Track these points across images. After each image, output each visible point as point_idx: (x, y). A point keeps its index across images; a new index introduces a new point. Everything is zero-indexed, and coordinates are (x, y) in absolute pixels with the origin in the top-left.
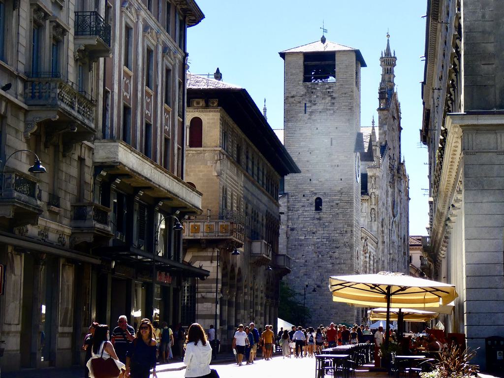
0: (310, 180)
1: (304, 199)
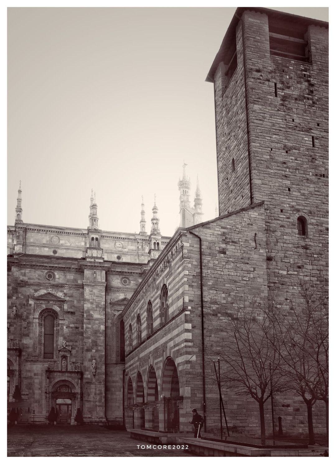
0: (289, 190)
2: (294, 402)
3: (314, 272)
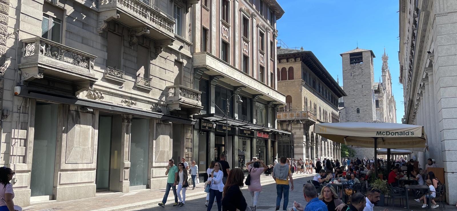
1: (352, 109)
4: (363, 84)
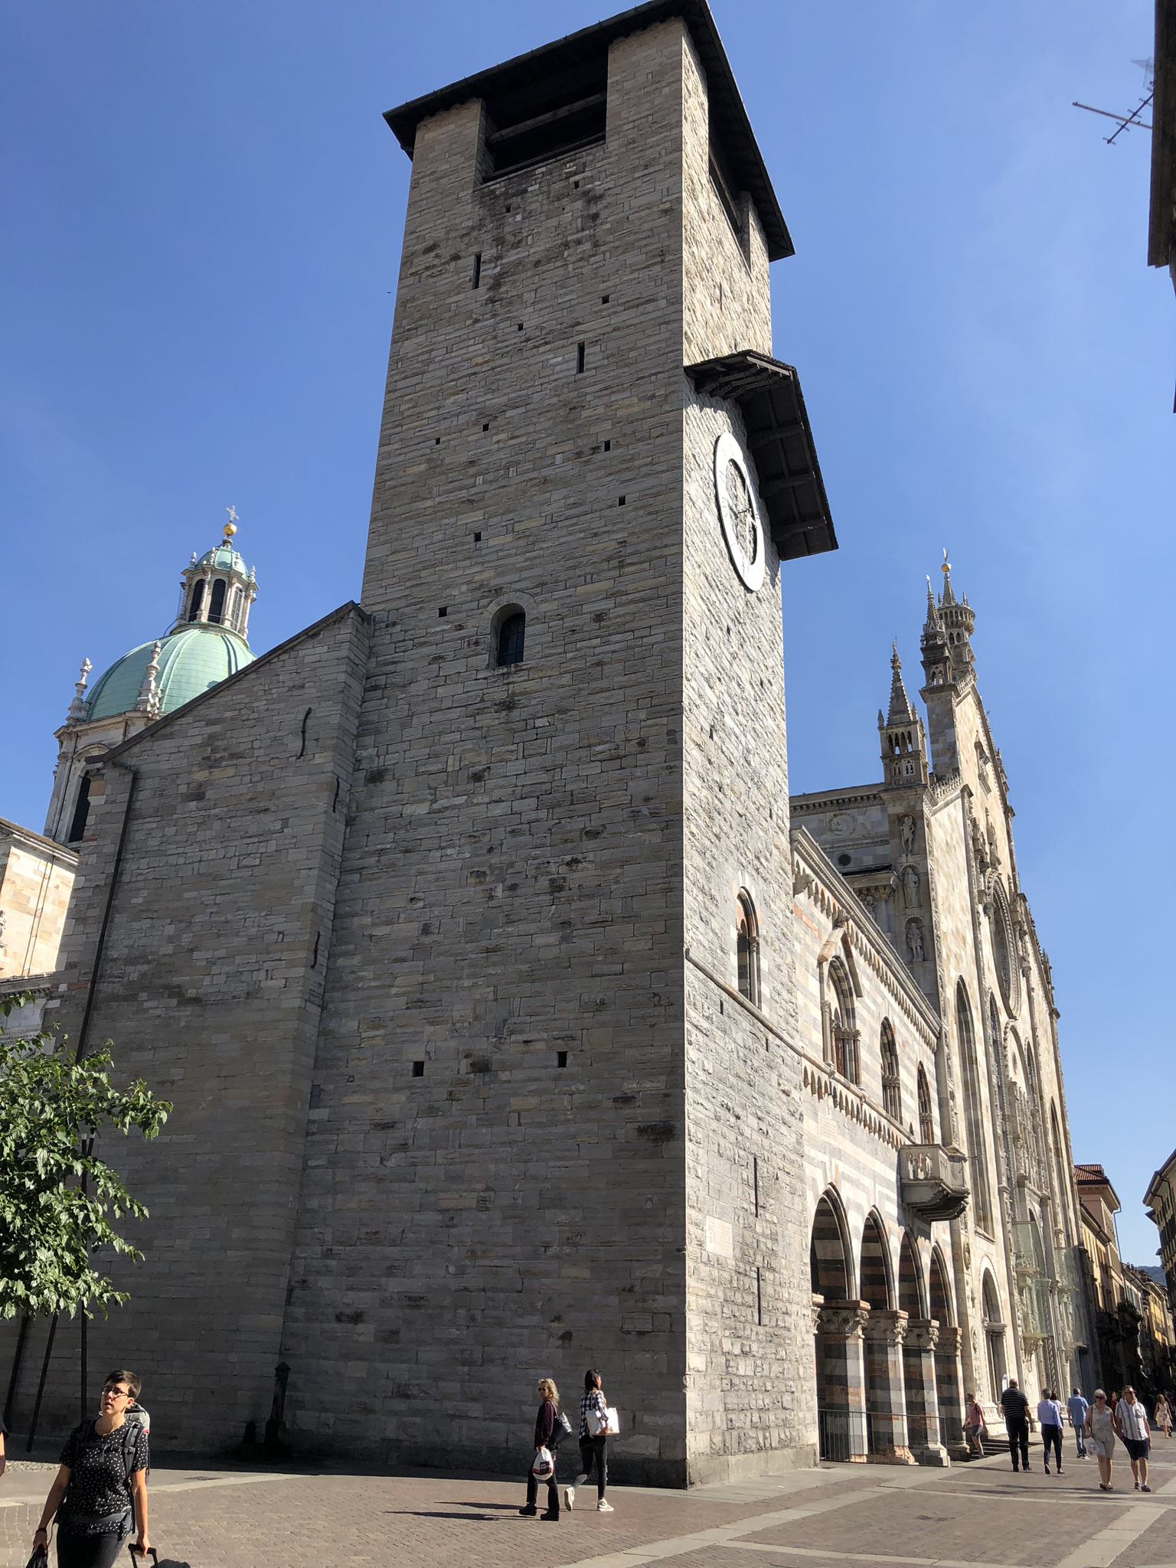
0: (478, 537)
2: (384, 1303)
3: (530, 779)
4: (589, 330)
